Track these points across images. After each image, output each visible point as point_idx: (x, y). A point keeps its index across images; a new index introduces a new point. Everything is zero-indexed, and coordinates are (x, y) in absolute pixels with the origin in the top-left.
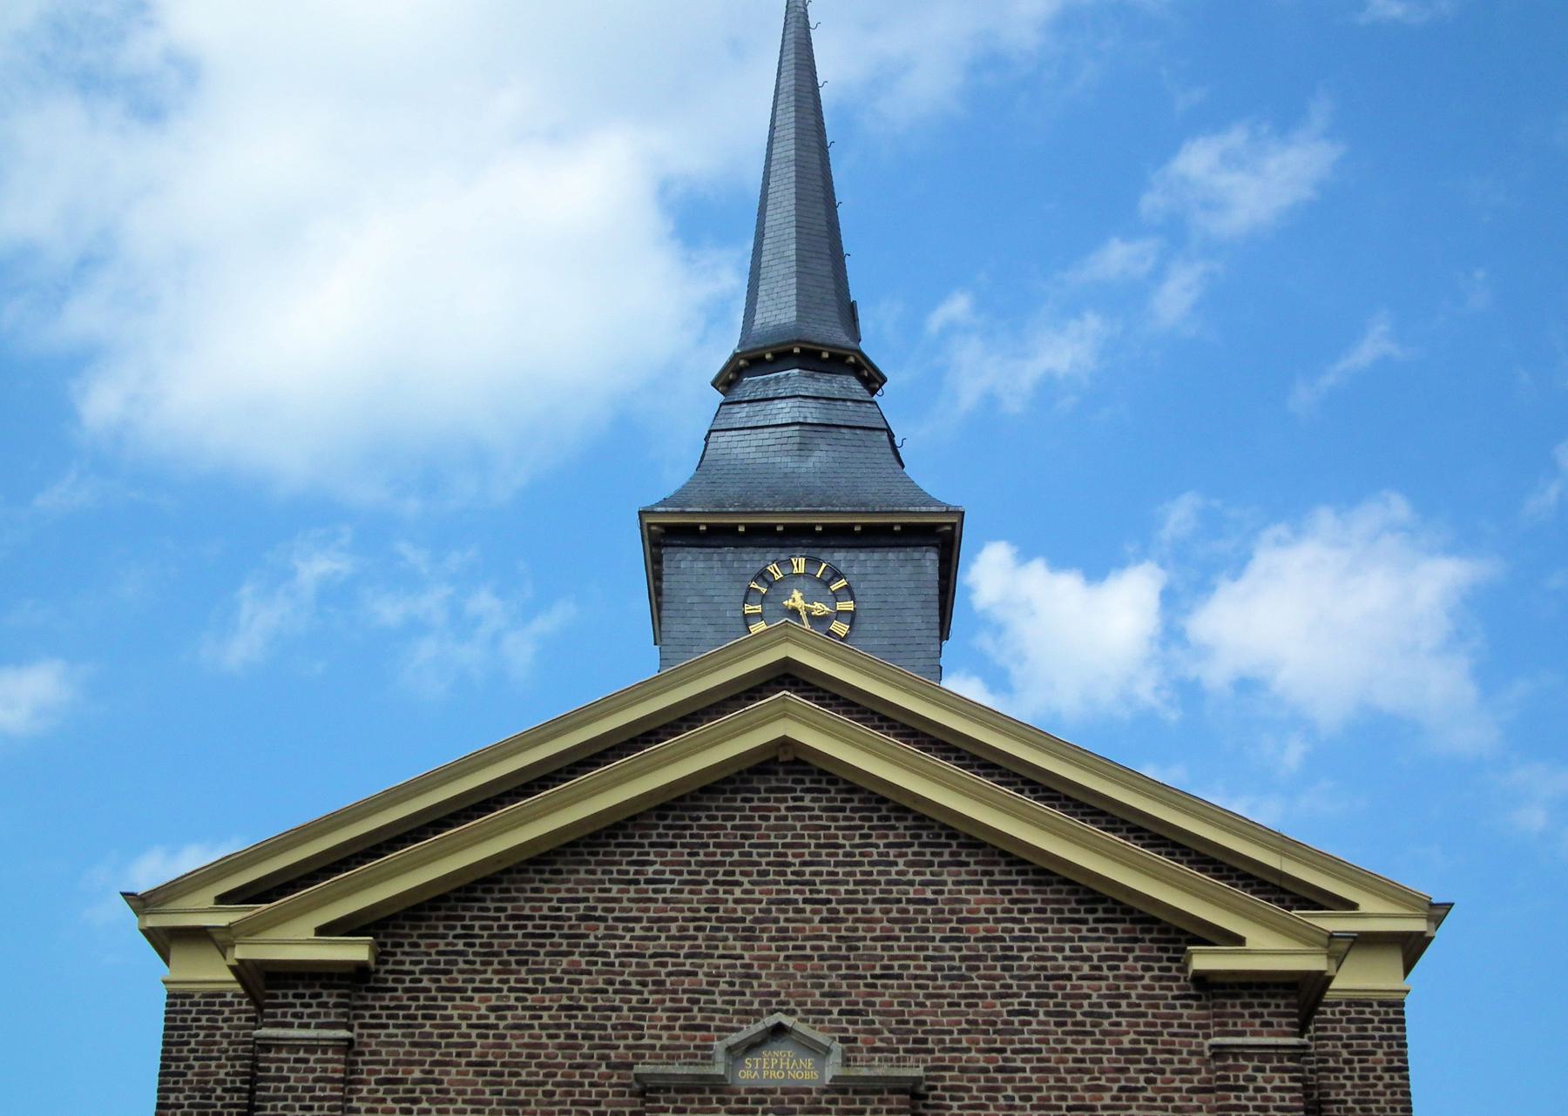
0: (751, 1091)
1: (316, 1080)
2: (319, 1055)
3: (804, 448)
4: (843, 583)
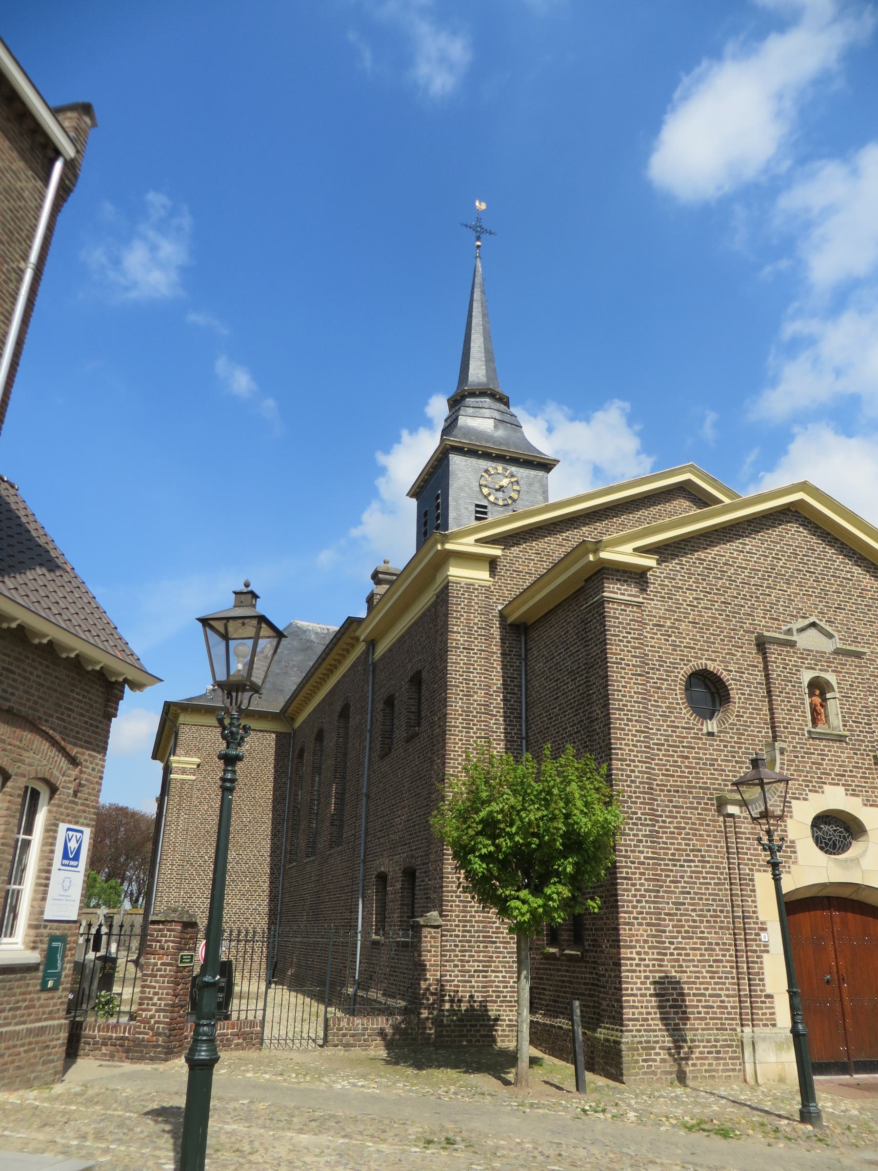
0: (805, 650)
1: (631, 620)
2: (630, 609)
3: (495, 426)
4: (515, 479)
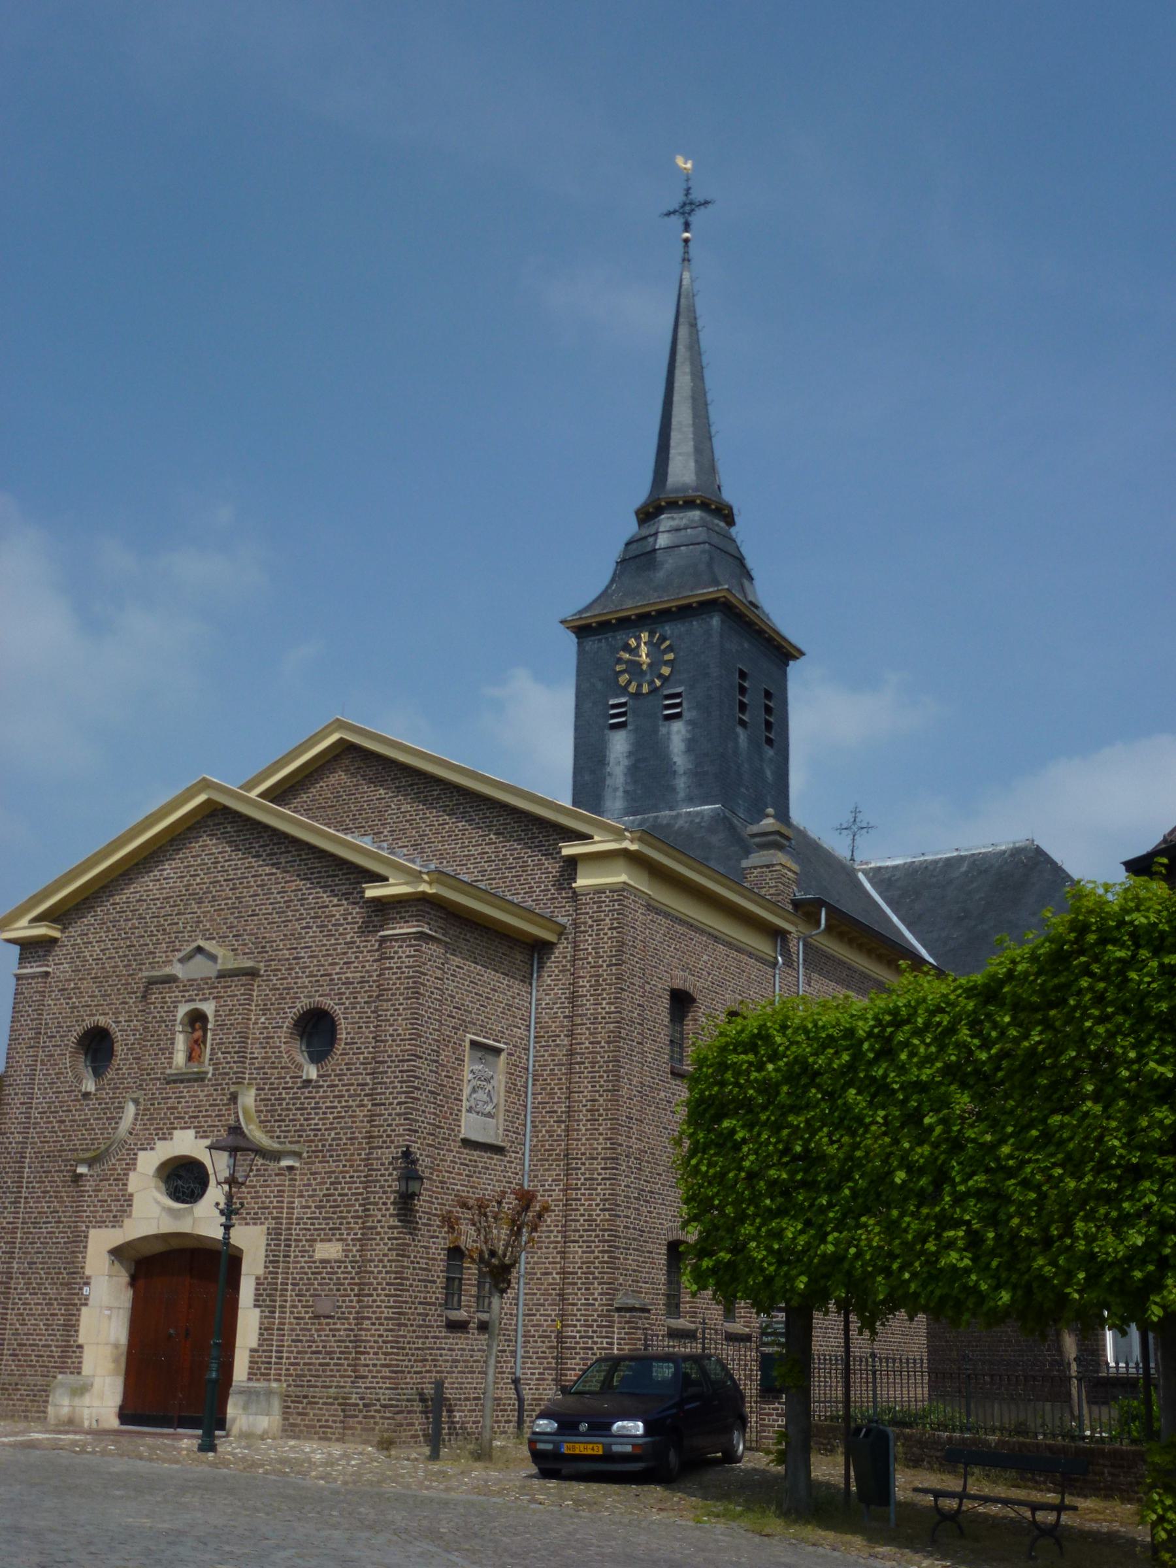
4: (668, 643)
